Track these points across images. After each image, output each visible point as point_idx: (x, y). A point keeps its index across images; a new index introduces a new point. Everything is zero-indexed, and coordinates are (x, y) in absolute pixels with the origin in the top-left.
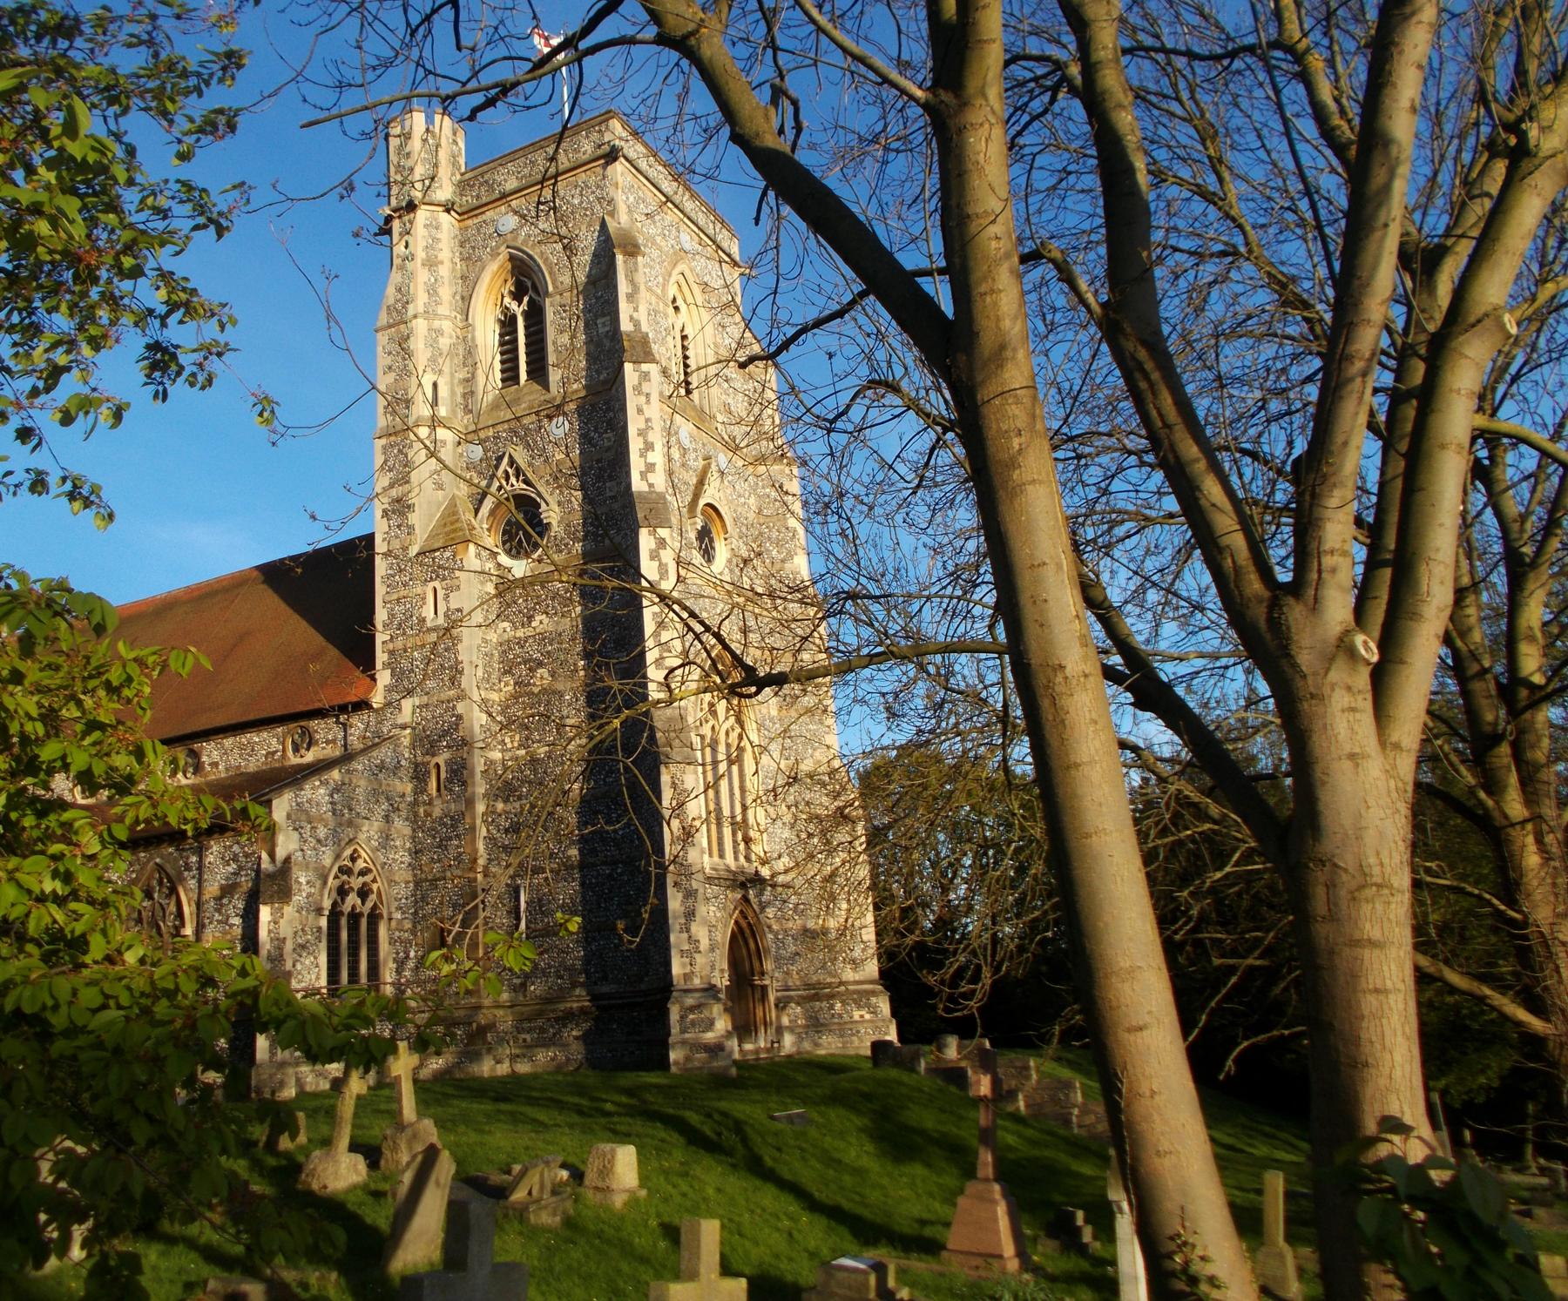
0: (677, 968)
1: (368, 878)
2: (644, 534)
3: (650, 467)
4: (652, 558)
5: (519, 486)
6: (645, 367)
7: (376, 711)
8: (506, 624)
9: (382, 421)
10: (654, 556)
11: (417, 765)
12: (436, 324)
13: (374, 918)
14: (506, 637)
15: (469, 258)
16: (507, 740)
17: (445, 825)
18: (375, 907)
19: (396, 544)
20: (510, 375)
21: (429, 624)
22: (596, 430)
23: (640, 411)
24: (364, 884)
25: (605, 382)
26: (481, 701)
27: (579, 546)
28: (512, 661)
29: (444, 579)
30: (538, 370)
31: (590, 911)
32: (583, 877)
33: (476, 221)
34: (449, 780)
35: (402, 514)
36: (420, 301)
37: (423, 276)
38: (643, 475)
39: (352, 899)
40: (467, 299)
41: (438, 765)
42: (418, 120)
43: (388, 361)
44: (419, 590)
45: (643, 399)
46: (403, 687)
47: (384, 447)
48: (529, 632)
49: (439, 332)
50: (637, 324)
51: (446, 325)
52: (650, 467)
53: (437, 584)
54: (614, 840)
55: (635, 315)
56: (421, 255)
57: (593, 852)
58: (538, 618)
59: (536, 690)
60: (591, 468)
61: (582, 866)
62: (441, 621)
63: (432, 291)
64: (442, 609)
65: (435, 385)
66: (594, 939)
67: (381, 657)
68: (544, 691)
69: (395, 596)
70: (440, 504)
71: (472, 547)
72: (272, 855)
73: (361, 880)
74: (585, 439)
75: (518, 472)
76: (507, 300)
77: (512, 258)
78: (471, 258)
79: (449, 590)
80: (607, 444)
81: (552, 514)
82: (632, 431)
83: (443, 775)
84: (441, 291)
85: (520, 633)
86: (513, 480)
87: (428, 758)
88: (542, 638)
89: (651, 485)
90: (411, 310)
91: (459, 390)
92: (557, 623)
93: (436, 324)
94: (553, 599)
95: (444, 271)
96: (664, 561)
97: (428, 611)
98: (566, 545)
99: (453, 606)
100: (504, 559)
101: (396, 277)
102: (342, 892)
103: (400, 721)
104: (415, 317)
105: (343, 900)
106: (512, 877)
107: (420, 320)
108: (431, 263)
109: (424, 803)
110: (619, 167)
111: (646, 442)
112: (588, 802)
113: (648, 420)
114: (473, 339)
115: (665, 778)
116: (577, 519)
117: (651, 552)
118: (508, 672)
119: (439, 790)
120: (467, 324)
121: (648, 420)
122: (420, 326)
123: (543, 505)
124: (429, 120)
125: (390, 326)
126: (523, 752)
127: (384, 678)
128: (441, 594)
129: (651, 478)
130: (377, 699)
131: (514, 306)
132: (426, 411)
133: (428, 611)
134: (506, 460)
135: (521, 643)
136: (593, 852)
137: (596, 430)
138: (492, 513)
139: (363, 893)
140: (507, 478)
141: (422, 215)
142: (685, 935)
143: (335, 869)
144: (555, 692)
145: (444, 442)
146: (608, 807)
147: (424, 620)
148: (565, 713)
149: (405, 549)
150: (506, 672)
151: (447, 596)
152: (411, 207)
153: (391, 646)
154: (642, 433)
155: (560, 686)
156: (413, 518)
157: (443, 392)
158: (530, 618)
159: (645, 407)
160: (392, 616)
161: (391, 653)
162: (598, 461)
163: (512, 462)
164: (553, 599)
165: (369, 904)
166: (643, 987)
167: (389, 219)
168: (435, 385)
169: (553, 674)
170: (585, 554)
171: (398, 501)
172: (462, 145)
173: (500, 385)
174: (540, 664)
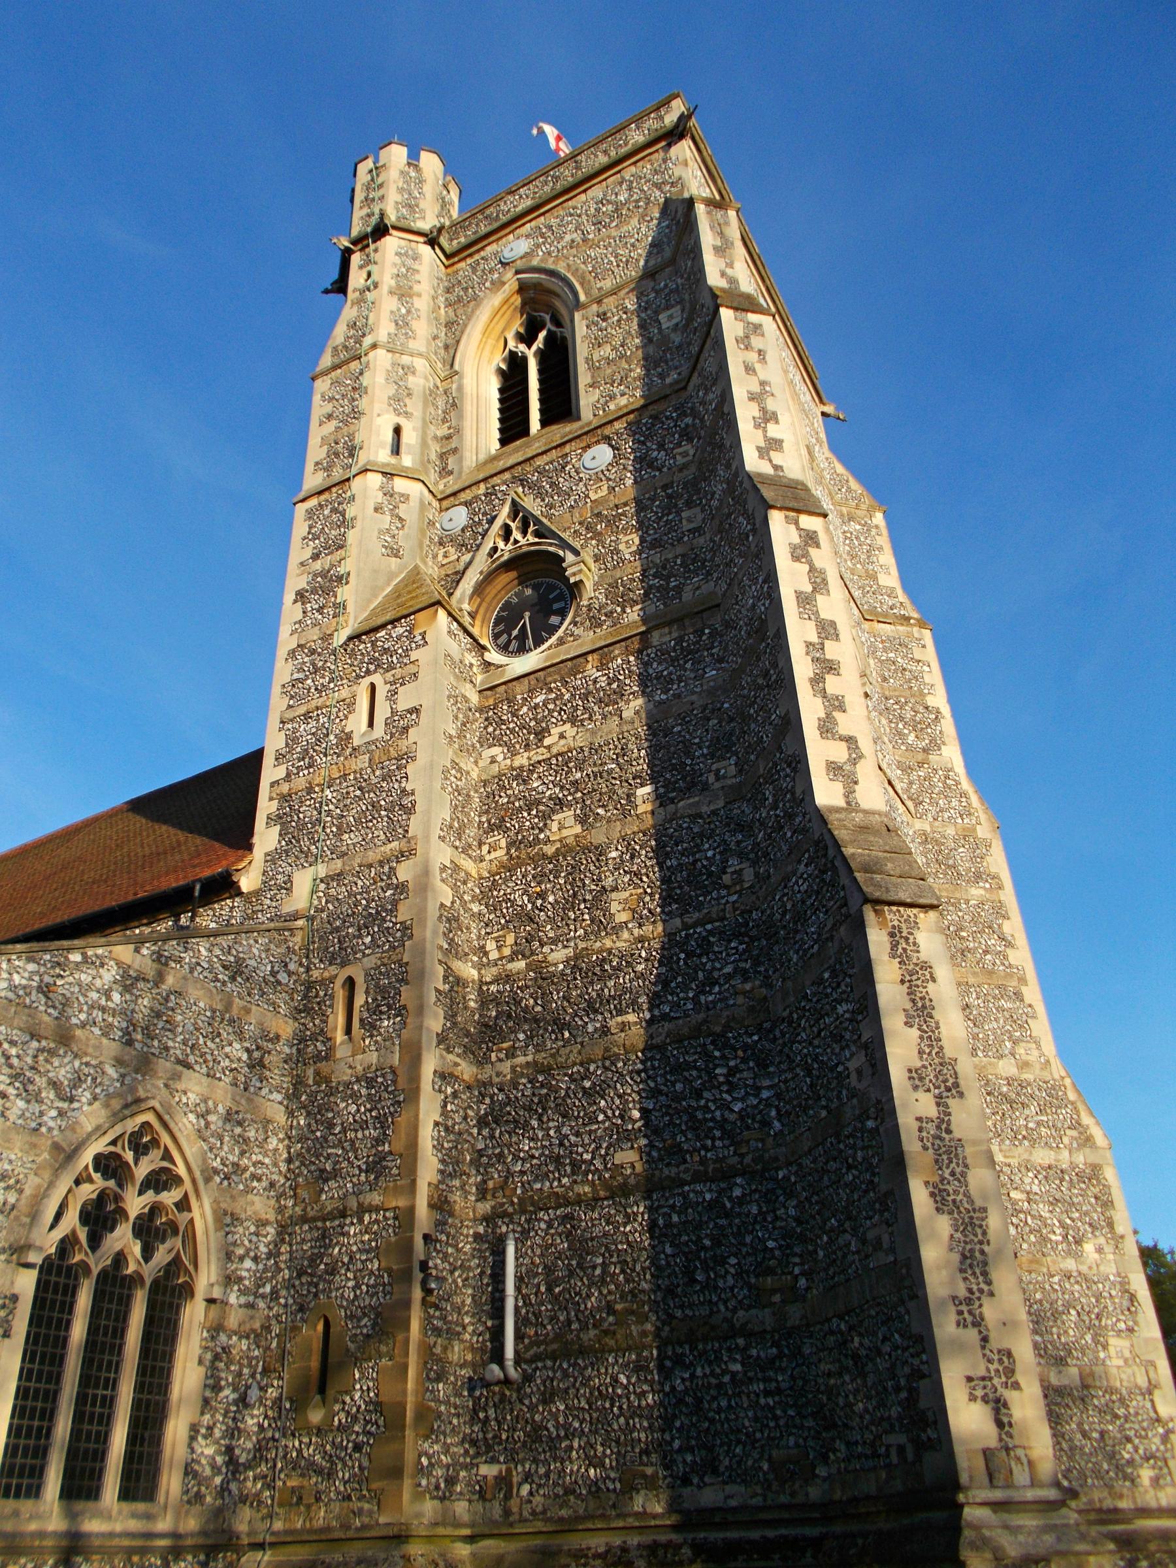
1: (169, 1198)
2: (776, 519)
3: (775, 444)
4: (796, 558)
5: (525, 541)
7: (248, 898)
8: (496, 750)
9: (313, 480)
10: (799, 554)
11: (309, 985)
12: (406, 360)
13: (170, 1292)
14: (495, 769)
15: (459, 300)
16: (491, 945)
17: (355, 1096)
18: (175, 1266)
19: (314, 634)
20: (513, 425)
21: (356, 741)
22: (661, 447)
23: (749, 369)
24: (155, 1209)
25: (677, 382)
26: (444, 859)
27: (633, 615)
28: (504, 809)
29: (391, 667)
31: (670, 1292)
32: (650, 1209)
33: (469, 261)
34: (374, 1010)
35: (328, 591)
36: (384, 330)
37: (388, 305)
38: (763, 453)
39: (122, 1238)
40: (451, 349)
42: (397, 154)
43: (328, 408)
44: (345, 693)
45: (753, 357)
46: (298, 840)
47: (310, 514)
48: (539, 754)
49: (409, 370)
50: (733, 281)
51: (420, 364)
52: (775, 444)
53: (377, 679)
54: (722, 1124)
55: (729, 271)
56: (387, 281)
57: (675, 1152)
58: (555, 731)
59: (550, 850)
60: (653, 499)
61: (651, 1187)
62: (379, 731)
63: (402, 323)
64: (383, 711)
65: (397, 431)
66: (679, 1361)
67: (266, 806)
68: (565, 850)
69: (302, 710)
70: (391, 576)
71: (442, 614)
73: (150, 1196)
74: (643, 462)
76: (511, 344)
77: (523, 288)
78: (459, 302)
79: (396, 685)
80: (680, 460)
81: (585, 571)
82: (740, 392)
83: (360, 1000)
84: (415, 324)
85: (522, 760)
86: (516, 535)
87: (333, 970)
88: (564, 760)
89: (777, 468)
90: (368, 341)
91: (435, 449)
92: (593, 733)
93: (406, 360)
94: (585, 697)
95: (422, 304)
96: (818, 564)
97: (357, 723)
98: (609, 615)
99: (403, 705)
100: (494, 656)
101: (349, 312)
102: (100, 1217)
103: (287, 908)
104: (374, 346)
105: (95, 1241)
106: (488, 1219)
107: (380, 352)
108: (403, 293)
109: (318, 1058)
111: (763, 410)
112: (661, 1048)
113: (763, 384)
114: (460, 388)
115: (877, 939)
116: (632, 570)
117: (794, 548)
118: (498, 826)
119: (348, 1031)
121: (763, 384)
122: (380, 359)
123: (570, 558)
124: (414, 157)
125: (335, 367)
126: (521, 964)
127: (266, 838)
129: (777, 458)
130: (247, 883)
131: (522, 347)
132: (383, 456)
133: (357, 723)
134: (506, 510)
135: (522, 776)
136: (675, 1152)
137: (661, 447)
138: (479, 590)
139: (149, 1230)
140: (507, 533)
141: (391, 243)
142: (972, 1334)
143: (87, 1158)
144: (586, 849)
145: (406, 498)
146: (708, 1056)
147: (349, 736)
148: (609, 882)
149: (327, 638)
150: (492, 828)
151: (392, 695)
152: (381, 231)
153: (285, 788)
155: (598, 836)
156: (344, 593)
157: (410, 437)
158: (541, 734)
159: (758, 366)
160: (292, 740)
161: (285, 798)
162: (665, 487)
163: (516, 509)
164: (585, 697)
165: (162, 1256)
166: (814, 1493)
167: (346, 254)
168: (397, 431)
169: (582, 820)
170: (644, 620)
171: (324, 574)
172: (454, 196)
173: (498, 446)
174: (560, 804)
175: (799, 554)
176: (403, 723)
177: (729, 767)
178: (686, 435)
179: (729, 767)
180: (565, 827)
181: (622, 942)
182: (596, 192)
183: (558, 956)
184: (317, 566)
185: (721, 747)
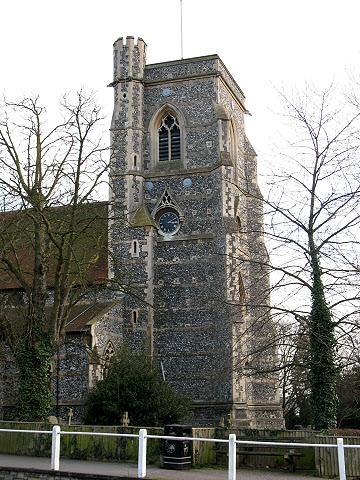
0: (235, 395)
6: (229, 168)
20: (163, 155)
30: (177, 154)
41: (135, 313)
52: (230, 208)
53: (136, 240)
72: (90, 345)
75: (169, 199)
97: (132, 251)
100: (160, 232)
110: (219, 82)
120: (146, 133)
128: (138, 245)
131: (166, 127)
133: (132, 251)
154: (227, 194)
155: (183, 286)
157: (139, 160)
158: (172, 258)
163: (166, 195)
175: (231, 243)
176: (144, 255)
177: (211, 278)
178: (210, 186)
179: (211, 278)
180: (176, 282)
181: (188, 310)
182: (191, 82)
183: (175, 310)
184: (117, 200)
185: (211, 273)
